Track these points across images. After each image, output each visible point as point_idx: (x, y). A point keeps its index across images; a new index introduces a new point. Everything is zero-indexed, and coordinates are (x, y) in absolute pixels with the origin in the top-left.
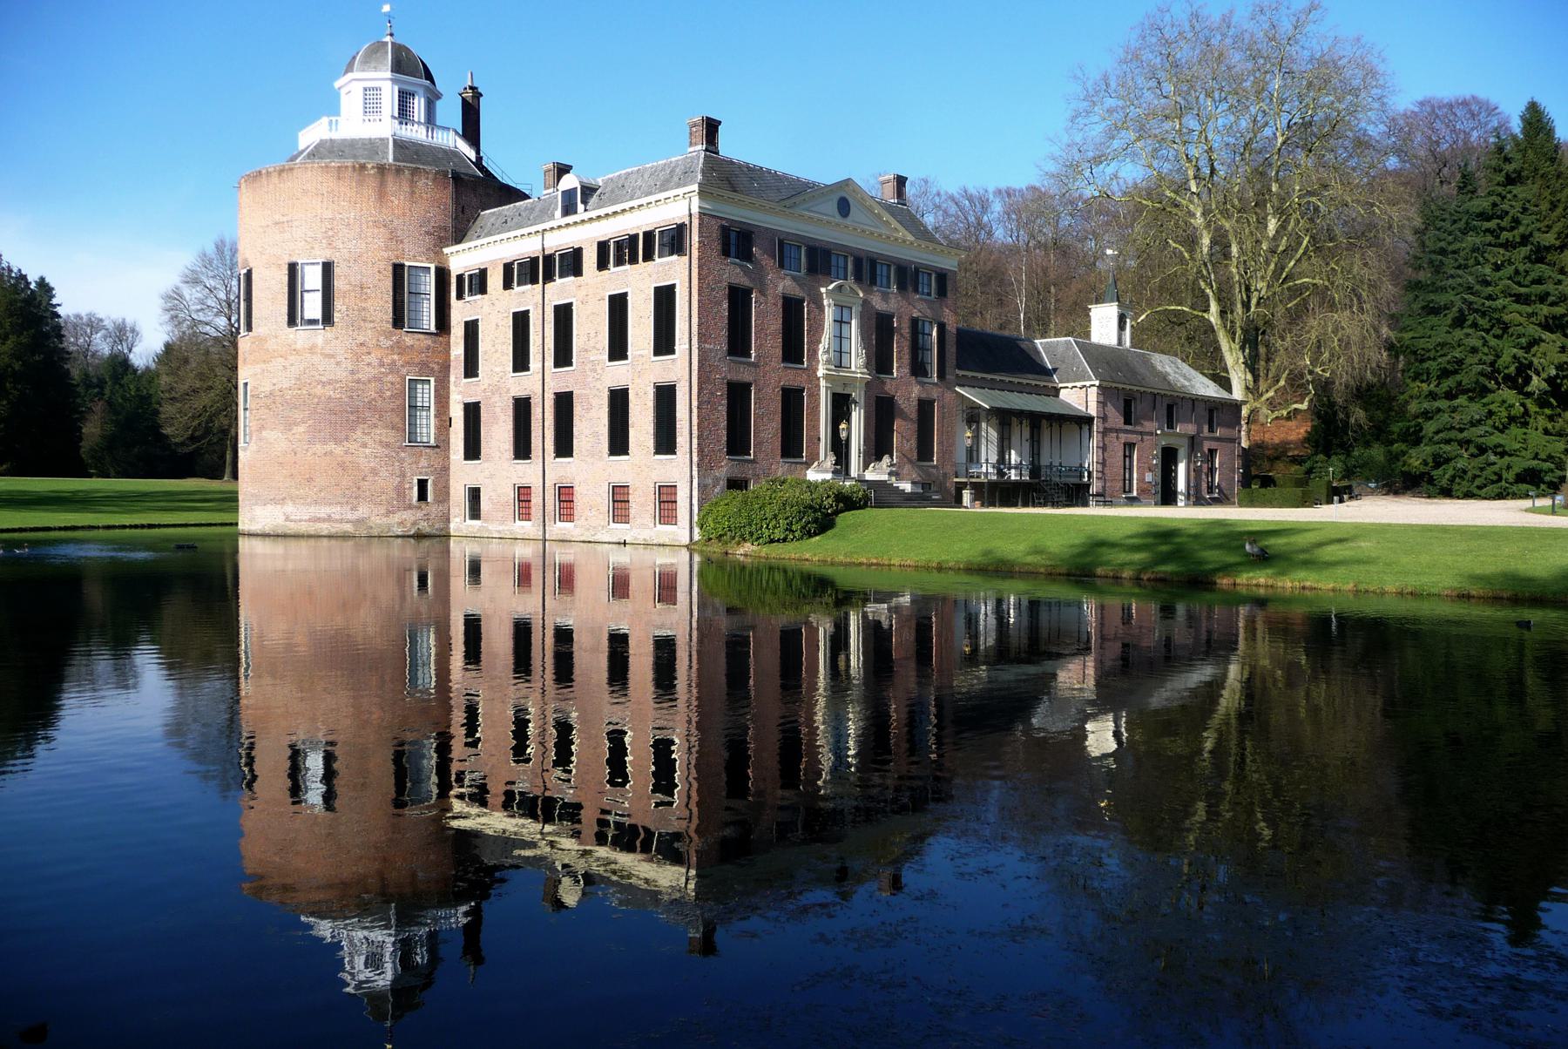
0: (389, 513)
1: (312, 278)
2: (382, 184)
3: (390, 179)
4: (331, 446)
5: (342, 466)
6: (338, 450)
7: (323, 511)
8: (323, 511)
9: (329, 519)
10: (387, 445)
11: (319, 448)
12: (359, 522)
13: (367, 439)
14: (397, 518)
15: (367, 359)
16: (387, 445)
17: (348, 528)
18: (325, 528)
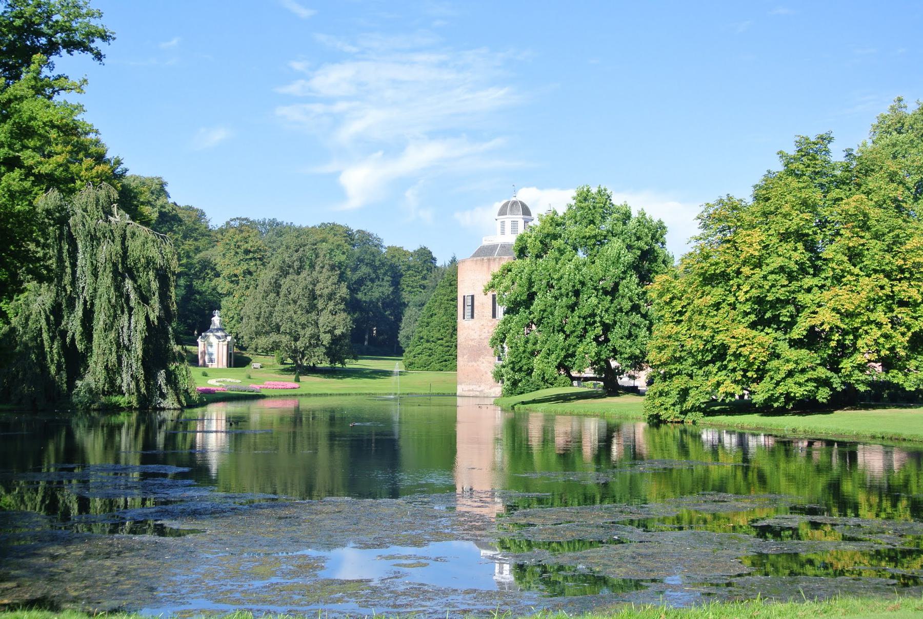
0: (491, 388)
1: (469, 302)
2: (489, 265)
3: (492, 262)
4: (473, 363)
5: (476, 370)
6: (475, 364)
7: (471, 387)
8: (471, 387)
9: (473, 390)
10: (490, 363)
11: (470, 364)
12: (482, 391)
13: (484, 360)
14: (493, 390)
15: (484, 330)
16: (490, 363)
17: (478, 393)
18: (471, 394)
